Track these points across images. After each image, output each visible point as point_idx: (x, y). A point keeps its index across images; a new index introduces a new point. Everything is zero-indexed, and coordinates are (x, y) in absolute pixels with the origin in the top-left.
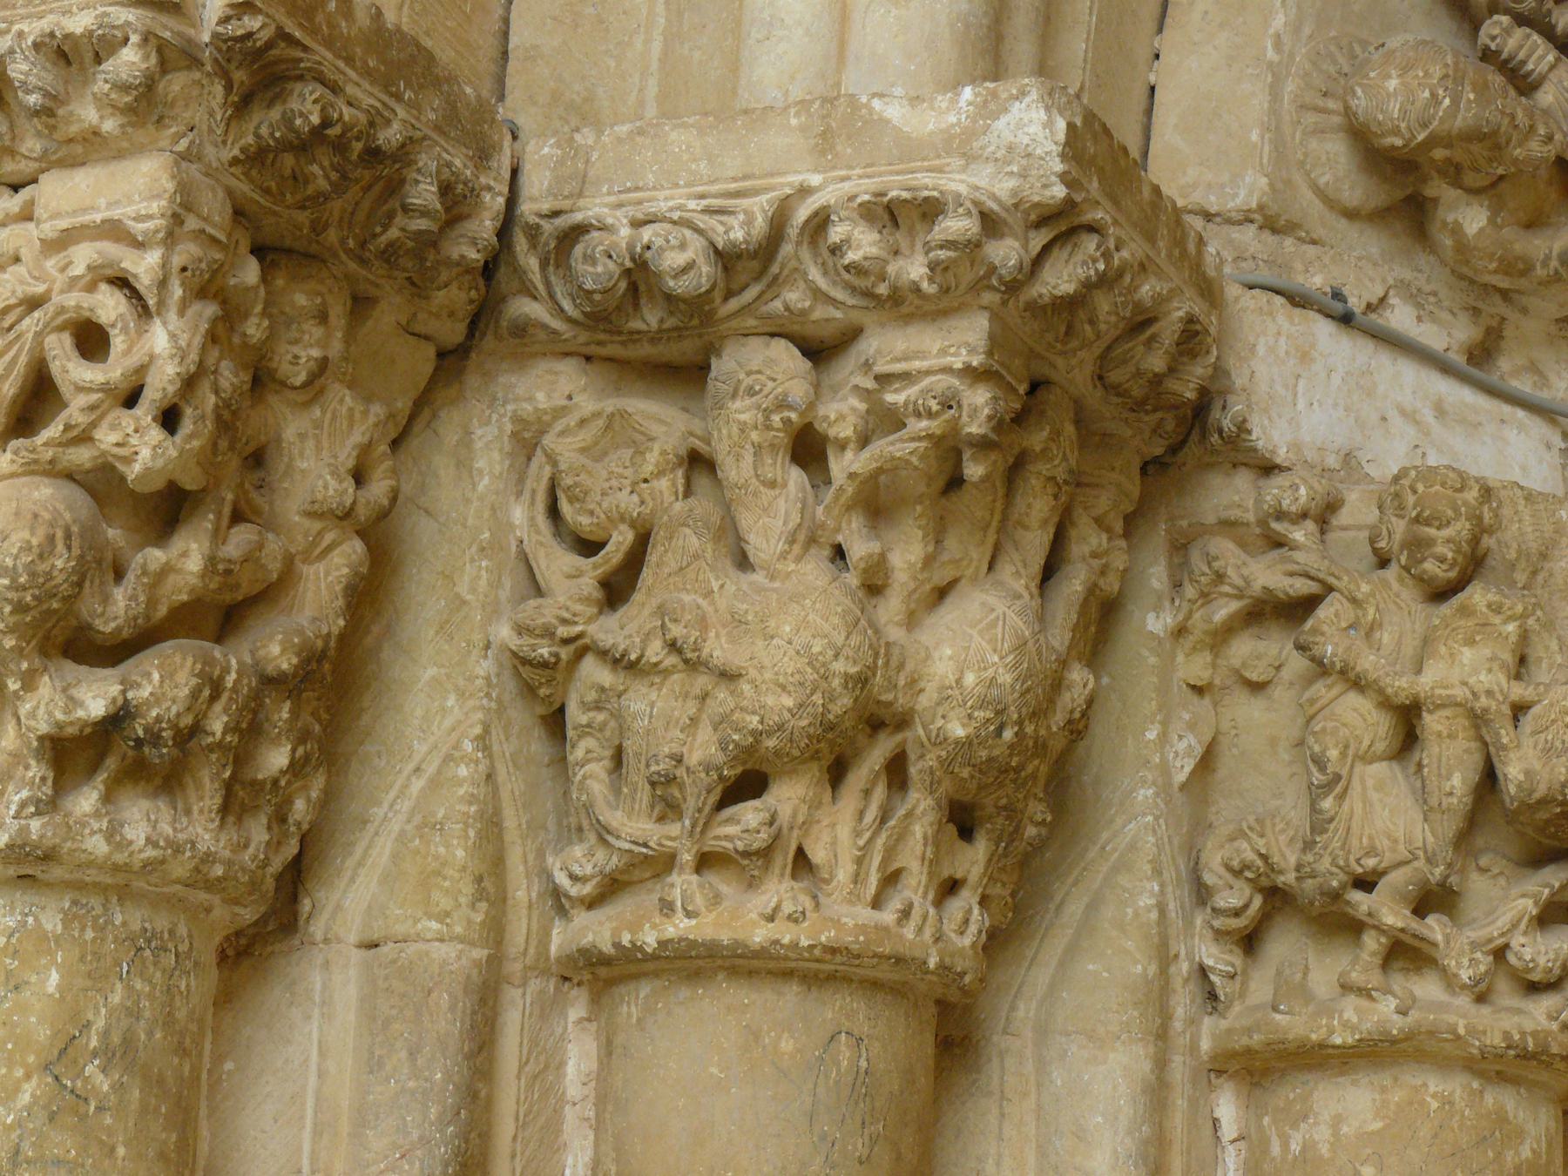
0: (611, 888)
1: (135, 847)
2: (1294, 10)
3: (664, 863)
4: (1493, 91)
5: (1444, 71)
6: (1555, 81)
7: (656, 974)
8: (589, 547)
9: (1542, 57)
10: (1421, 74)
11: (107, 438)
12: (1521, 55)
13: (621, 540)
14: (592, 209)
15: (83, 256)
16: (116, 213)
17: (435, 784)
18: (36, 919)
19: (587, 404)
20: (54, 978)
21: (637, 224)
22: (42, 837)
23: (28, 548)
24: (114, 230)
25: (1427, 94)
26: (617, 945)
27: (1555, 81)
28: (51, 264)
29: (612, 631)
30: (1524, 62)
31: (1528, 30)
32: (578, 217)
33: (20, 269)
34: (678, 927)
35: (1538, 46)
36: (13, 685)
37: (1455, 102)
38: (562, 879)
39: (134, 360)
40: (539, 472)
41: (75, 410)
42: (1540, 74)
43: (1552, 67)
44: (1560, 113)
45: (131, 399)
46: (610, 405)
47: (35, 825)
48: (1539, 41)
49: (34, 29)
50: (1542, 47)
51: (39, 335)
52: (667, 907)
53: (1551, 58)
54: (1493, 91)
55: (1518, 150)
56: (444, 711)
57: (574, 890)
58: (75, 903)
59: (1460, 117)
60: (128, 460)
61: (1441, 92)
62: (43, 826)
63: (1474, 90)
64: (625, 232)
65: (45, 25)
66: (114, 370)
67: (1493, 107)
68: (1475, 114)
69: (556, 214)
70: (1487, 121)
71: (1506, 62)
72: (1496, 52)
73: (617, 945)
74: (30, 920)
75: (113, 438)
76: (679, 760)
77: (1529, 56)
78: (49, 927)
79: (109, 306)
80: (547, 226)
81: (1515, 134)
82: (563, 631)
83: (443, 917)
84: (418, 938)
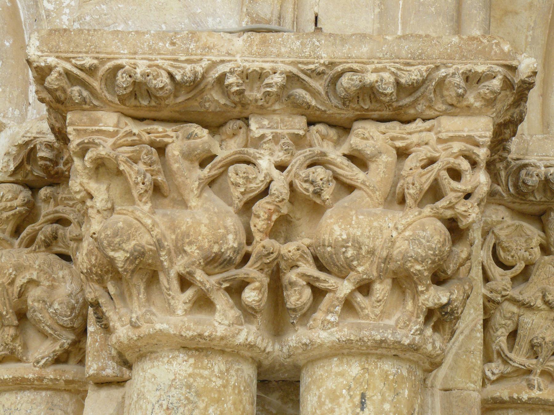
0: (502, 378)
1: (437, 349)
3: (529, 372)
7: (516, 408)
8: (505, 267)
11: (460, 208)
13: (520, 267)
14: (532, 159)
15: (457, 147)
16: (472, 134)
17: (469, 337)
18: (401, 371)
19: (509, 221)
20: (406, 392)
21: (546, 167)
22: (419, 342)
23: (439, 242)
24: (470, 140)
26: (511, 398)
28: (440, 147)
29: (514, 293)
32: (527, 162)
33: (428, 147)
34: (535, 394)
36: (421, 288)
38: (489, 374)
39: (474, 184)
40: (491, 240)
41: (451, 196)
45: (468, 196)
46: (517, 222)
47: (417, 338)
49: (463, 68)
51: (439, 170)
52: (531, 386)
56: (470, 314)
57: (493, 378)
58: (410, 366)
60: (465, 217)
62: (419, 338)
64: (543, 168)
65: (468, 67)
66: (463, 186)
69: (518, 159)
73: (511, 398)
74: (399, 371)
75: (463, 209)
76: (544, 339)
78: (404, 374)
79: (465, 165)
80: (513, 163)
82: (504, 293)
83: (475, 383)
84: (468, 389)
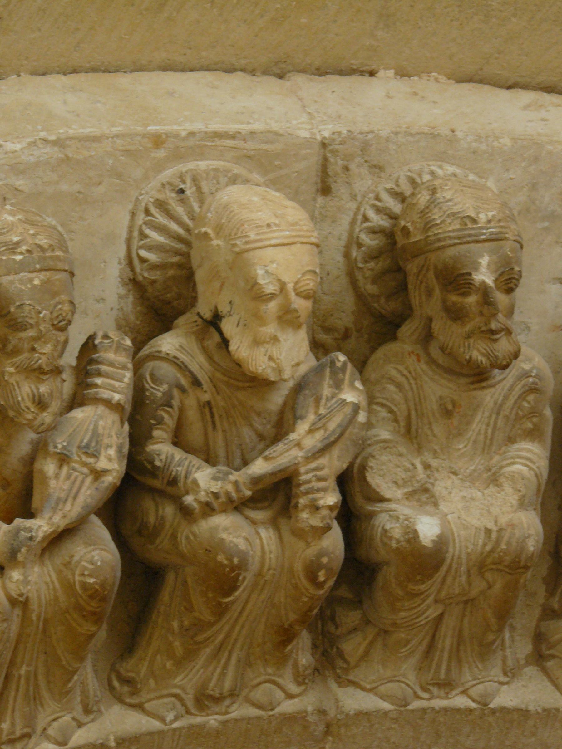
2: (32, 159)
4: (53, 302)
5: (46, 247)
6: (99, 412)
9: (114, 390)
10: (32, 232)
12: (104, 368)
25: (15, 239)
27: (99, 412)
30: (99, 374)
31: (130, 366)
35: (121, 381)
37: (22, 267)
42: (97, 393)
43: (108, 403)
44: (71, 430)
48: (126, 380)
50: (123, 385)
53: (117, 397)
54: (53, 302)
55: (12, 370)
59: (10, 278)
61: (24, 248)
63: (44, 283)
67: (38, 307)
68: (22, 291)
70: (21, 305)
71: (92, 361)
72: (95, 346)
77: (106, 375)
81: (26, 355)
